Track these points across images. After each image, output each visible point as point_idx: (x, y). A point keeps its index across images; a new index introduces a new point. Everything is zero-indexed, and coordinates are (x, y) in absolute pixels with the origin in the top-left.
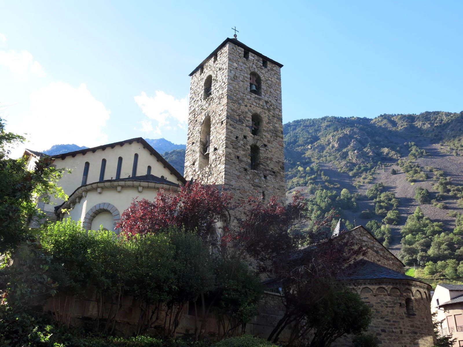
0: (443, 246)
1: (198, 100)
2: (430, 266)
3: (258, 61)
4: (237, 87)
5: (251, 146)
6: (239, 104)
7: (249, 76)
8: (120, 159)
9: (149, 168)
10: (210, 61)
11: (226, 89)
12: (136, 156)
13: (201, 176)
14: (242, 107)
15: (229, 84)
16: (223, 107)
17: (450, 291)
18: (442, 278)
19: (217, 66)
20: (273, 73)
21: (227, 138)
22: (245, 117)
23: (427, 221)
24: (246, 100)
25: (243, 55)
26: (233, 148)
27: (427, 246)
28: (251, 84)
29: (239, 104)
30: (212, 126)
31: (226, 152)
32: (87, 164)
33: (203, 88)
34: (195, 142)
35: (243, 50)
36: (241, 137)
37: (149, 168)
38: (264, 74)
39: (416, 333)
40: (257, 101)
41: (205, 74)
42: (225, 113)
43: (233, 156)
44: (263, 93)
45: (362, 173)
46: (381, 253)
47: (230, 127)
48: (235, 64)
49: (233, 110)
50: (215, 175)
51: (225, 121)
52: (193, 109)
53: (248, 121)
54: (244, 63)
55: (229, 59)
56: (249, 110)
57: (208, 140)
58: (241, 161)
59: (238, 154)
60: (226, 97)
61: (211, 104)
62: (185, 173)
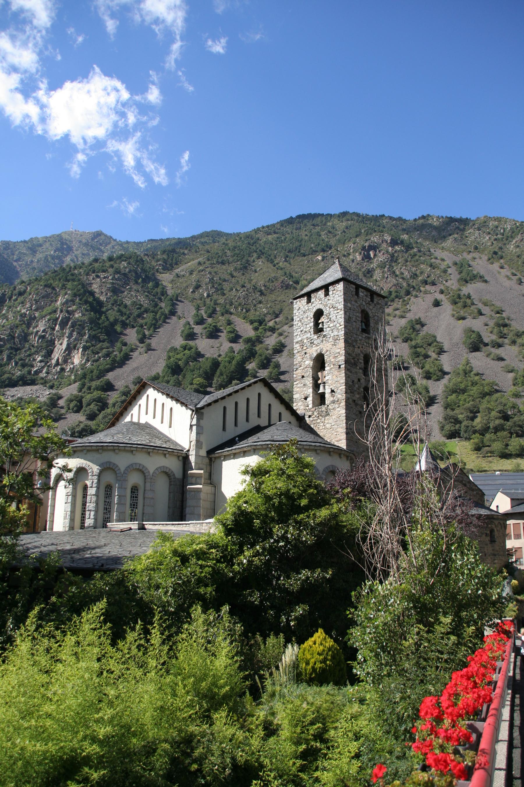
0: (494, 414)
1: (306, 332)
2: (476, 440)
3: (366, 296)
4: (351, 329)
5: (364, 388)
6: (354, 346)
7: (360, 315)
8: (248, 400)
9: (270, 405)
10: (320, 292)
11: (343, 332)
12: (259, 394)
13: (316, 414)
14: (356, 350)
15: (345, 327)
16: (339, 350)
17: (512, 500)
18: (489, 455)
19: (330, 302)
20: (379, 306)
21: (346, 384)
22: (358, 360)
23: (477, 378)
24: (359, 342)
25: (354, 293)
26: (351, 392)
27: (474, 413)
28: (362, 322)
29: (354, 346)
30: (326, 365)
31: (346, 397)
32: (225, 408)
33: (312, 320)
34: (305, 375)
35: (354, 287)
36: (356, 380)
37: (270, 405)
38: (372, 311)
39: (495, 555)
40: (367, 341)
41: (313, 305)
42: (343, 358)
43: (351, 400)
44: (371, 331)
45: (393, 301)
46: (468, 485)
47: (348, 372)
48: (349, 305)
49: (349, 354)
50: (334, 417)
51: (344, 366)
52: (300, 339)
53: (361, 363)
54: (356, 302)
55: (345, 300)
56: (361, 351)
57: (320, 376)
58: (356, 405)
59: (354, 398)
60: (343, 340)
61: (324, 342)
62: (294, 404)
